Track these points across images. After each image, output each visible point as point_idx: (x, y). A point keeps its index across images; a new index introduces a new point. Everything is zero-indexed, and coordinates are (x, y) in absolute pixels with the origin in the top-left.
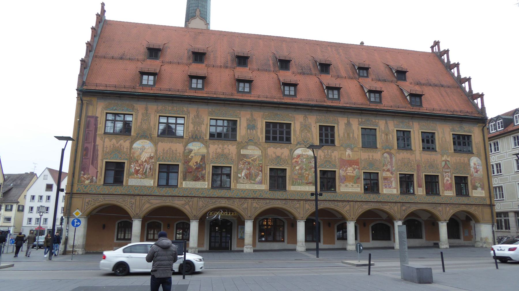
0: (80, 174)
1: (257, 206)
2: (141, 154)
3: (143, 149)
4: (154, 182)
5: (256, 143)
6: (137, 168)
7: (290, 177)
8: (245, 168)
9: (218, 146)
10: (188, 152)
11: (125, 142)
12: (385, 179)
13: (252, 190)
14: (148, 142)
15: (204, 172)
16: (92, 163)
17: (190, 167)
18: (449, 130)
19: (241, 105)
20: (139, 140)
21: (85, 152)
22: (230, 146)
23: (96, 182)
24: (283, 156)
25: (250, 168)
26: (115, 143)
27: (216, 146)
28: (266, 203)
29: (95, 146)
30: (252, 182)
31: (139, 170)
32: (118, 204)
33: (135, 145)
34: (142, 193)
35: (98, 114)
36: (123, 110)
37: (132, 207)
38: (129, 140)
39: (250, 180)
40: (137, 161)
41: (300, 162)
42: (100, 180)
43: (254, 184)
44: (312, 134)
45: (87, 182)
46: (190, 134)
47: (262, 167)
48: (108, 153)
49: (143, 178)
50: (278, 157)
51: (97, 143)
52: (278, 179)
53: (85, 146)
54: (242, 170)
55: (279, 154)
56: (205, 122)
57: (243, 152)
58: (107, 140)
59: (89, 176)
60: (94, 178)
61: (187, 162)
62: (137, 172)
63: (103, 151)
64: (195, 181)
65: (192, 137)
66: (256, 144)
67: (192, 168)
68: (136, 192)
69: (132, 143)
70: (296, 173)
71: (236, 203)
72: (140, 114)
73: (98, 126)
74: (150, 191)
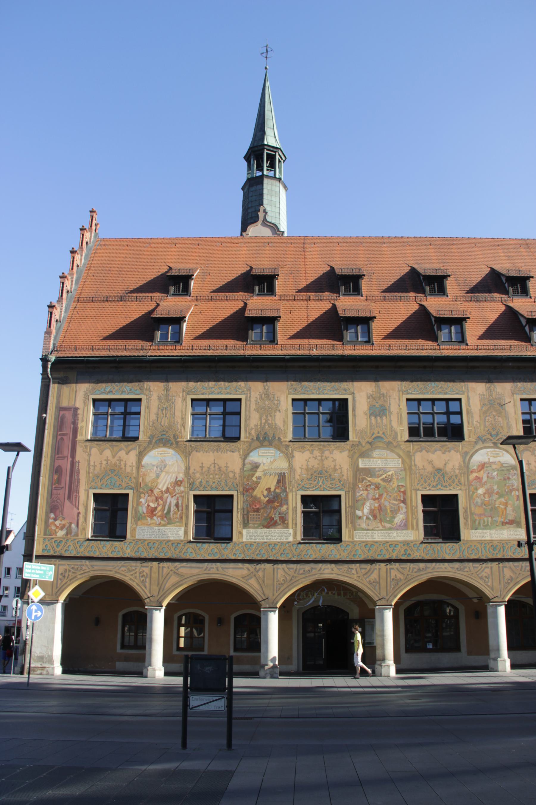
0: (47, 518)
1: (399, 576)
2: (158, 476)
3: (162, 466)
4: (186, 533)
5: (389, 443)
6: (152, 505)
7: (466, 511)
8: (370, 496)
9: (312, 453)
10: (251, 470)
11: (127, 453)
13: (387, 542)
14: (171, 451)
15: (284, 508)
16: (69, 497)
17: (256, 500)
20: (153, 448)
21: (56, 477)
22: (335, 452)
23: (77, 535)
24: (448, 469)
25: (381, 495)
26: (110, 458)
27: (307, 454)
28: (419, 570)
29: (73, 464)
30: (388, 525)
31: (156, 508)
32: (118, 576)
33: (146, 460)
34: (162, 556)
35: (79, 404)
37: (143, 582)
38: (135, 449)
39: (381, 521)
40: (152, 491)
41: (485, 479)
42: (84, 529)
43: (390, 529)
44: (506, 418)
45: (61, 533)
46: (253, 432)
47: (404, 493)
48: (97, 476)
49: (164, 525)
50: (439, 470)
51: (77, 459)
52: (442, 516)
53: (56, 465)
54: (364, 501)
55: (439, 464)
57: (362, 463)
58: (95, 451)
59: (63, 522)
60: (73, 526)
61: (248, 490)
62: (152, 512)
64: (268, 527)
65: (258, 439)
66: (390, 446)
68: (153, 554)
69: (141, 455)
70: (479, 501)
71: (354, 571)
73: (79, 426)
74: (178, 550)
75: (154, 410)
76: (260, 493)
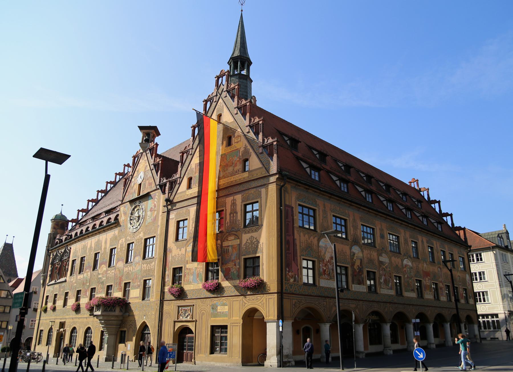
0: (286, 270)
2: (325, 253)
6: (324, 268)
11: (314, 238)
12: (441, 288)
16: (294, 260)
18: (457, 253)
19: (376, 214)
23: (298, 282)
35: (293, 205)
36: (309, 204)
37: (324, 310)
61: (353, 265)
63: (300, 246)
64: (359, 284)
69: (319, 241)
72: (321, 210)
75: (321, 218)
76: (356, 267)
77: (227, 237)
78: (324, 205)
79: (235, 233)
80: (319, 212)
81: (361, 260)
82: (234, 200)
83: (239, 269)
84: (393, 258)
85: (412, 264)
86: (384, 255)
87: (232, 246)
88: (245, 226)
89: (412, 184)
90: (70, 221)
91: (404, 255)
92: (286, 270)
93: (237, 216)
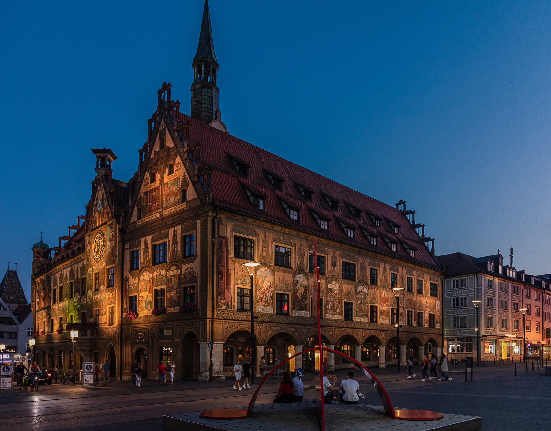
0: (217, 298)
6: (262, 296)
14: (268, 270)
16: (227, 288)
29: (227, 269)
35: (228, 236)
37: (259, 333)
45: (224, 307)
50: (349, 292)
56: (306, 256)
67: (298, 297)
76: (298, 294)
77: (170, 267)
78: (265, 234)
79: (176, 263)
80: (258, 242)
81: (306, 287)
82: (175, 231)
83: (180, 297)
84: (345, 286)
85: (368, 291)
86: (333, 282)
87: (174, 276)
88: (185, 257)
89: (399, 206)
90: (52, 249)
91: (360, 282)
92: (217, 298)
93: (177, 246)
